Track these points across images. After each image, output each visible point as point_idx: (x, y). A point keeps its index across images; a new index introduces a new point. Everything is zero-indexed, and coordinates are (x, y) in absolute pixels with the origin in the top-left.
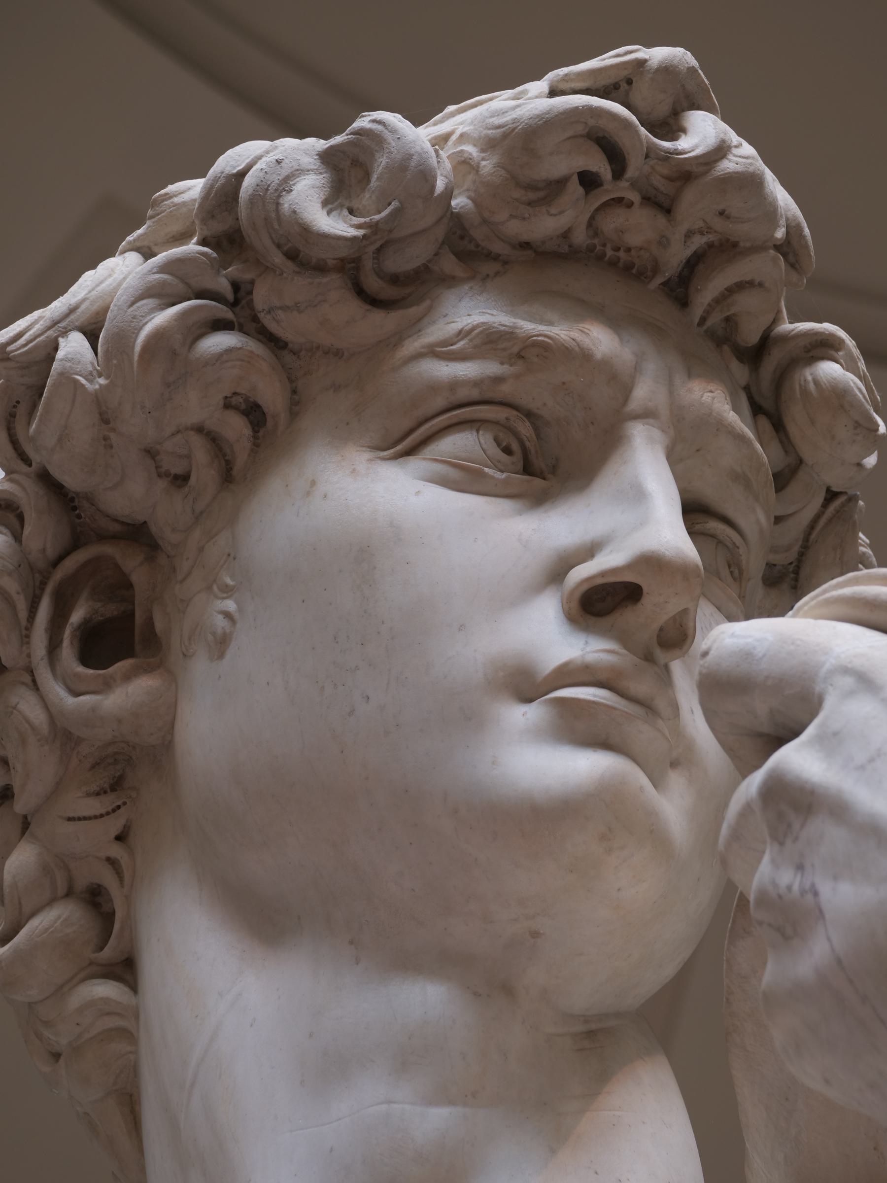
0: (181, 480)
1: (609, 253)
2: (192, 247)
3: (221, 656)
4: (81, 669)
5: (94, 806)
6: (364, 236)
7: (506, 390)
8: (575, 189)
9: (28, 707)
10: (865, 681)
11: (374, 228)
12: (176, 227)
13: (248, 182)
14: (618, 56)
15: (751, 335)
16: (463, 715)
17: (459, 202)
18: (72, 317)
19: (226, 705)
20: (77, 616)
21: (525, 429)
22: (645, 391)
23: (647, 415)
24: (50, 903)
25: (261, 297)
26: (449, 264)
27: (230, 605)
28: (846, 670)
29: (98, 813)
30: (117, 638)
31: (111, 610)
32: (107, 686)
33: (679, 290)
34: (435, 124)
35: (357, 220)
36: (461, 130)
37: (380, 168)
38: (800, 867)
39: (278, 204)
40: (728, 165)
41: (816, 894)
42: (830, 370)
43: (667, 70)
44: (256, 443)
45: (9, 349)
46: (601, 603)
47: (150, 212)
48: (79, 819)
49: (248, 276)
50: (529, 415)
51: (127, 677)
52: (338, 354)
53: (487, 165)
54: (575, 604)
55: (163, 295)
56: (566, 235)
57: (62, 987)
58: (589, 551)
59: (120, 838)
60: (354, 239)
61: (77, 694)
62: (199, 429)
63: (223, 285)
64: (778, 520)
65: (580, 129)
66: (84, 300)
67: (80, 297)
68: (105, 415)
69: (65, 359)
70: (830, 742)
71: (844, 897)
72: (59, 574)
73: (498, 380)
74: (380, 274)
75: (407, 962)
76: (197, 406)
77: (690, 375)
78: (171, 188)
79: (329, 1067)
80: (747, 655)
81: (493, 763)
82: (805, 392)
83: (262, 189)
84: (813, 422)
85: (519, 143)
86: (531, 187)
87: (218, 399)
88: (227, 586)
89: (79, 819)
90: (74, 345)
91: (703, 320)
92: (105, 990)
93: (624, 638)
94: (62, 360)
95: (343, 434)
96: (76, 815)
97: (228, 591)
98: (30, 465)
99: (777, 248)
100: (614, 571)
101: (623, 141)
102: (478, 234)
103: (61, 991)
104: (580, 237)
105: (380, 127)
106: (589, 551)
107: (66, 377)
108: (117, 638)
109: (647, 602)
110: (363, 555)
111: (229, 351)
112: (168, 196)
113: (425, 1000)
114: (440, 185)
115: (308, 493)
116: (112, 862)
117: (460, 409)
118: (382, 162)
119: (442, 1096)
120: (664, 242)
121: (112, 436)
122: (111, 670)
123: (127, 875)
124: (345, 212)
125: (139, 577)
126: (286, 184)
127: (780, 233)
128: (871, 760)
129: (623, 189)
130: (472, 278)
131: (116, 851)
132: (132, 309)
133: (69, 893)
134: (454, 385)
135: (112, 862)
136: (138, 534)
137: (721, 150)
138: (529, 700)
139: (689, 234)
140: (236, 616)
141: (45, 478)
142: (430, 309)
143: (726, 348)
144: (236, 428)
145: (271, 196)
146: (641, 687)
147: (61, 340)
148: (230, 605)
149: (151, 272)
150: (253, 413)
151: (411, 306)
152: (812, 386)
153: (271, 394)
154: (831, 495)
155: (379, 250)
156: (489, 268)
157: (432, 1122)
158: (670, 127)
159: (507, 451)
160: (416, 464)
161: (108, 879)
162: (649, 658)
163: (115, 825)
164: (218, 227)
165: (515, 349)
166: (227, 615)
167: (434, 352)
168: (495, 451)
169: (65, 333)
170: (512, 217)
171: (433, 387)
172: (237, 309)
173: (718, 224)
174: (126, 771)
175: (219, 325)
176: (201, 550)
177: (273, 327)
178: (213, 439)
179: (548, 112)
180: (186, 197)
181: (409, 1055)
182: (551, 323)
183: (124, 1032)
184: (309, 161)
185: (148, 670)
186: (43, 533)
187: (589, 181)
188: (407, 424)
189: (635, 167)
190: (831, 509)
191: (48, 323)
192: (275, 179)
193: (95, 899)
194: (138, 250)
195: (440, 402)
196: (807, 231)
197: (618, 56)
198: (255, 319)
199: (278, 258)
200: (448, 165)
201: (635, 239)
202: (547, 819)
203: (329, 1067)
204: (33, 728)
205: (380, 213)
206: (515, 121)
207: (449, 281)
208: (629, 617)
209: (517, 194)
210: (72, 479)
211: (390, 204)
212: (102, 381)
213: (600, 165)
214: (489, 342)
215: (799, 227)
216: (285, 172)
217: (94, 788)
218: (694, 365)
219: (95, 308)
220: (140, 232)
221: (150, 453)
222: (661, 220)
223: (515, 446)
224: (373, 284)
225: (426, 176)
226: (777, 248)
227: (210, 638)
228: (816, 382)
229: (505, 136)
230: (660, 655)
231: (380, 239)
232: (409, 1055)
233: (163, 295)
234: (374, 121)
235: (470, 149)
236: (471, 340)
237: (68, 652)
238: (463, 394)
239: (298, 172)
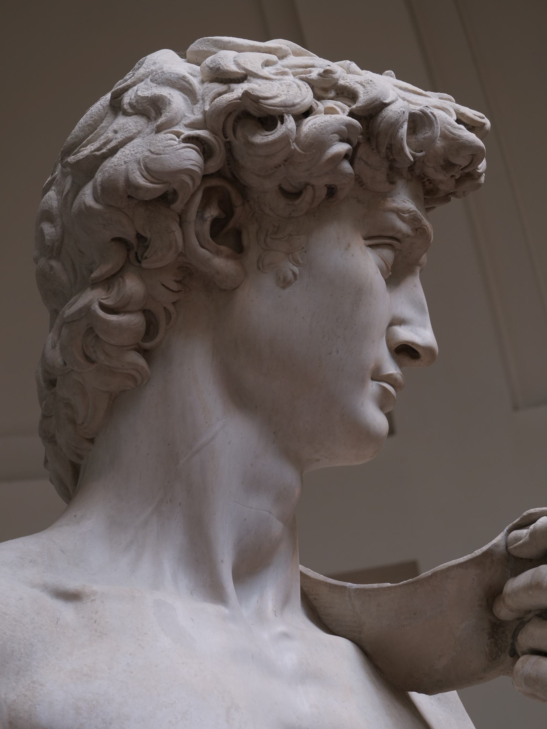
1: (425, 180)
3: (284, 288)
4: (210, 239)
5: (174, 286)
9: (178, 234)
12: (326, 86)
14: (480, 117)
18: (292, 108)
25: (361, 151)
27: (296, 269)
29: (171, 288)
32: (218, 253)
37: (427, 135)
45: (261, 101)
46: (405, 352)
48: (166, 288)
49: (361, 141)
51: (228, 257)
54: (396, 347)
57: (124, 346)
58: (401, 322)
59: (173, 303)
61: (203, 247)
62: (313, 186)
63: (355, 143)
66: (298, 104)
67: (298, 101)
68: (289, 160)
73: (408, 236)
79: (254, 484)
81: (362, 404)
85: (456, 145)
88: (298, 261)
89: (166, 288)
90: (290, 122)
92: (141, 361)
94: (289, 130)
96: (166, 285)
97: (297, 263)
98: (226, 138)
100: (417, 345)
105: (432, 116)
109: (418, 362)
110: (358, 292)
115: (347, 249)
121: (282, 167)
122: (223, 248)
125: (238, 211)
132: (331, 135)
134: (399, 231)
136: (243, 190)
138: (373, 379)
140: (298, 277)
141: (229, 148)
145: (395, 125)
147: (286, 117)
148: (296, 269)
149: (342, 124)
157: (277, 528)
161: (162, 318)
165: (417, 227)
166: (294, 274)
169: (288, 113)
170: (434, 167)
171: (393, 228)
176: (290, 235)
179: (473, 143)
180: (336, 76)
184: (407, 116)
188: (376, 234)
191: (283, 105)
194: (309, 84)
195: (390, 234)
197: (480, 117)
199: (384, 150)
201: (442, 187)
206: (459, 136)
209: (442, 162)
211: (422, 151)
212: (294, 146)
214: (414, 221)
217: (178, 280)
219: (301, 110)
227: (282, 277)
229: (453, 139)
234: (432, 113)
236: (410, 216)
237: (207, 227)
238: (399, 236)
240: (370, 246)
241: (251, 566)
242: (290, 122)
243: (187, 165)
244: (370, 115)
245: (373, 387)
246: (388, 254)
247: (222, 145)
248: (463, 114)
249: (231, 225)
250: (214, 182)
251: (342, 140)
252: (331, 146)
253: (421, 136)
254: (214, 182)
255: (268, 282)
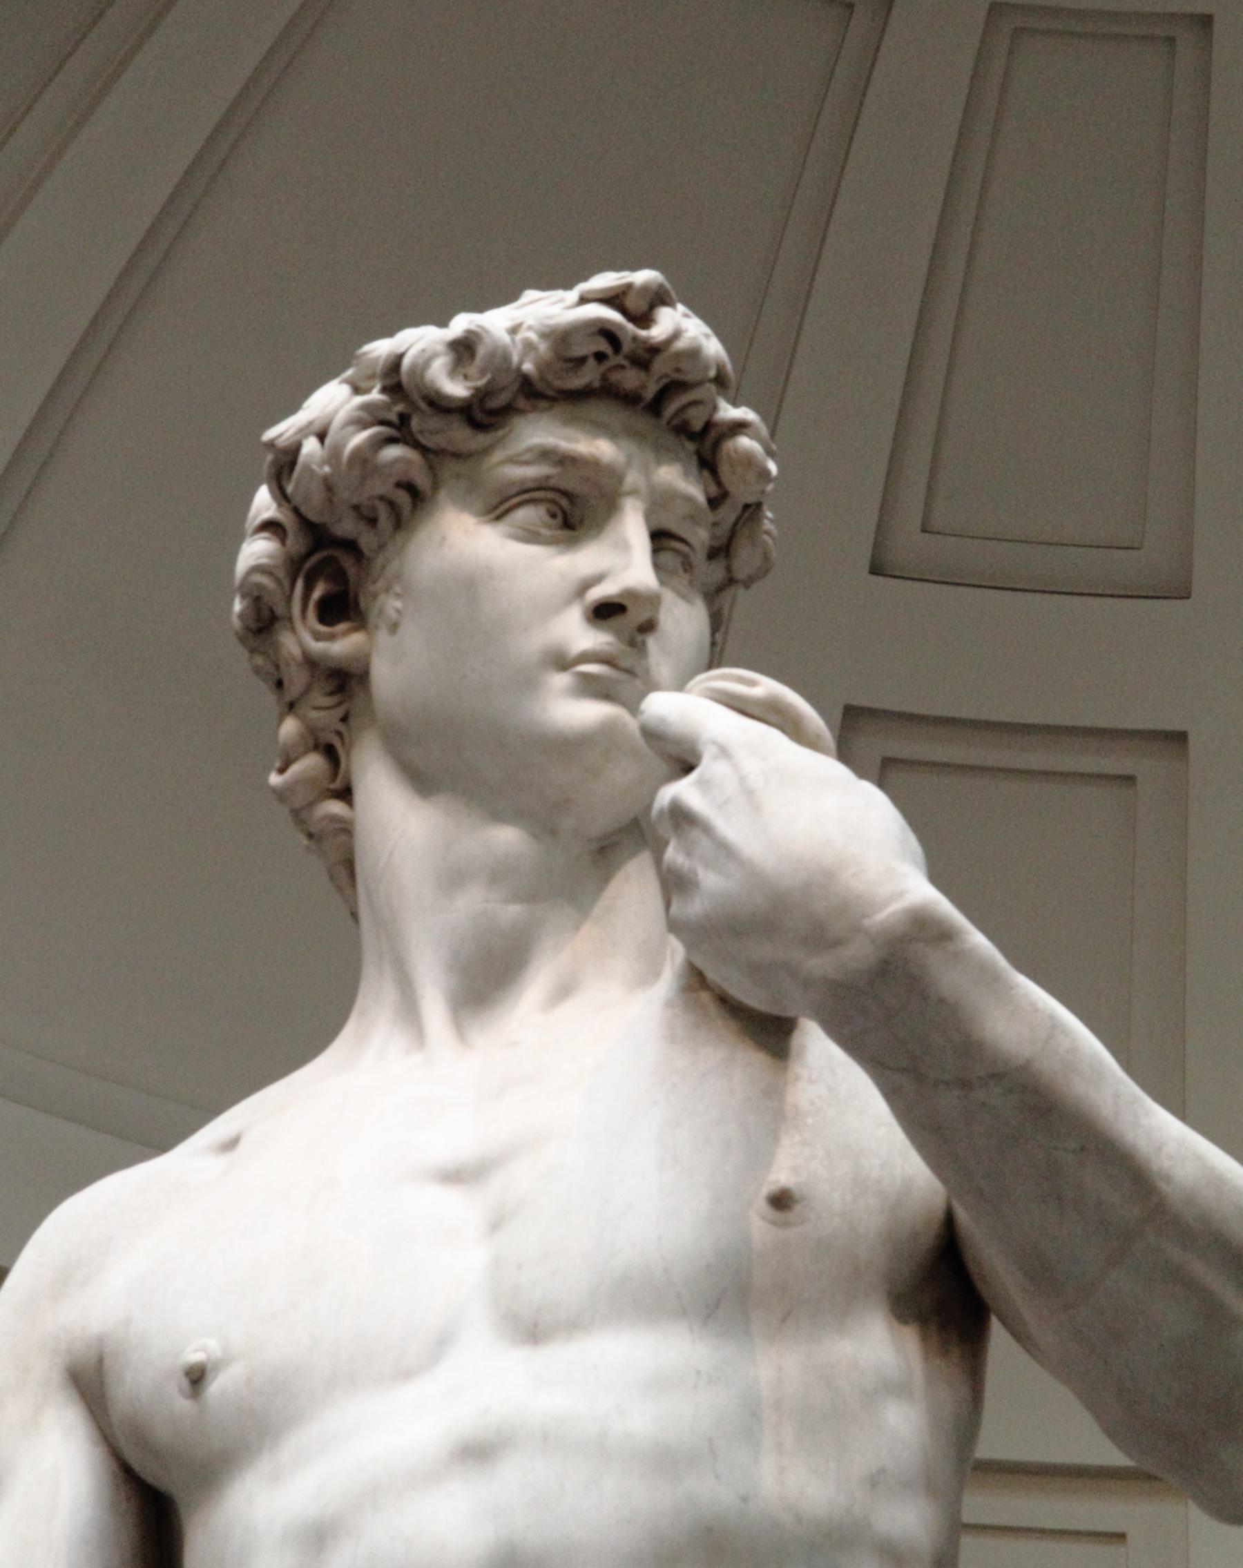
0: (372, 521)
2: (375, 395)
6: (473, 395)
7: (553, 483)
8: (591, 362)
10: (724, 752)
11: (477, 389)
13: (406, 362)
15: (697, 425)
16: (527, 682)
17: (528, 367)
19: (398, 658)
20: (317, 594)
21: (564, 502)
22: (633, 478)
23: (634, 492)
24: (305, 753)
25: (415, 423)
26: (521, 403)
27: (398, 604)
28: (715, 743)
30: (341, 608)
31: (335, 588)
32: (332, 637)
33: (655, 407)
34: (517, 308)
35: (469, 384)
36: (530, 321)
38: (689, 855)
39: (422, 376)
40: (681, 344)
41: (696, 875)
42: (745, 442)
43: (645, 288)
44: (415, 506)
46: (604, 612)
47: (355, 362)
50: (566, 494)
51: (346, 633)
52: (457, 455)
53: (543, 347)
55: (362, 424)
56: (588, 386)
58: (598, 579)
59: (344, 719)
60: (465, 400)
62: (382, 498)
63: (393, 417)
64: (714, 524)
65: (593, 329)
68: (329, 486)
69: (307, 455)
70: (705, 785)
71: (710, 880)
72: (308, 565)
73: (548, 478)
74: (483, 410)
75: (497, 816)
76: (380, 486)
77: (659, 463)
78: (367, 348)
79: (453, 879)
80: (663, 720)
82: (729, 457)
83: (414, 367)
84: (734, 472)
85: (561, 337)
86: (570, 360)
87: (392, 481)
90: (310, 446)
91: (668, 423)
92: (335, 807)
93: (618, 633)
95: (464, 504)
97: (398, 595)
99: (710, 381)
100: (611, 597)
101: (619, 334)
102: (540, 386)
103: (311, 804)
104: (596, 384)
106: (598, 579)
107: (307, 468)
108: (341, 608)
110: (471, 585)
111: (396, 461)
112: (365, 354)
113: (507, 838)
114: (515, 359)
116: (339, 734)
117: (528, 493)
118: (481, 351)
119: (516, 898)
120: (644, 387)
121: (335, 500)
123: (347, 741)
124: (461, 378)
126: (427, 363)
127: (712, 373)
128: (726, 802)
129: (619, 360)
130: (534, 408)
131: (341, 727)
133: (316, 747)
134: (523, 481)
135: (339, 734)
136: (351, 546)
137: (676, 335)
139: (657, 381)
142: (511, 431)
143: (683, 438)
144: (403, 498)
146: (626, 663)
150: (411, 489)
151: (496, 429)
152: (732, 453)
153: (422, 480)
154: (746, 507)
155: (482, 401)
156: (543, 404)
158: (644, 319)
159: (553, 516)
160: (502, 527)
162: (632, 643)
163: (339, 712)
164: (389, 382)
166: (398, 611)
167: (513, 460)
168: (547, 518)
169: (306, 436)
172: (400, 430)
173: (676, 376)
174: (346, 681)
175: (391, 441)
176: (383, 567)
177: (423, 441)
178: (391, 504)
181: (499, 874)
182: (578, 441)
183: (345, 829)
184: (440, 348)
185: (356, 629)
186: (296, 543)
187: (600, 357)
188: (494, 502)
189: (627, 347)
190: (746, 515)
192: (421, 361)
193: (330, 753)
196: (729, 367)
198: (411, 433)
199: (423, 405)
200: (520, 346)
202: (571, 746)
203: (453, 879)
204: (294, 659)
205: (480, 378)
207: (520, 412)
208: (617, 621)
210: (313, 516)
212: (327, 469)
213: (604, 346)
215: (724, 366)
216: (427, 355)
218: (662, 453)
220: (350, 372)
221: (356, 508)
222: (643, 375)
223: (559, 513)
224: (479, 415)
225: (506, 357)
226: (710, 381)
228: (736, 451)
230: (639, 638)
231: (482, 395)
232: (499, 874)
233: (359, 423)
235: (533, 336)
239: (435, 355)
240: (499, 518)
241: (487, 977)
242: (310, 446)
243: (252, 562)
244: (394, 377)
245: (561, 680)
246: (526, 515)
247: (290, 514)
248: (589, 292)
249: (352, 595)
250: (313, 560)
251: (364, 425)
252: (344, 445)
253: (478, 361)
254: (313, 560)
255: (383, 637)
